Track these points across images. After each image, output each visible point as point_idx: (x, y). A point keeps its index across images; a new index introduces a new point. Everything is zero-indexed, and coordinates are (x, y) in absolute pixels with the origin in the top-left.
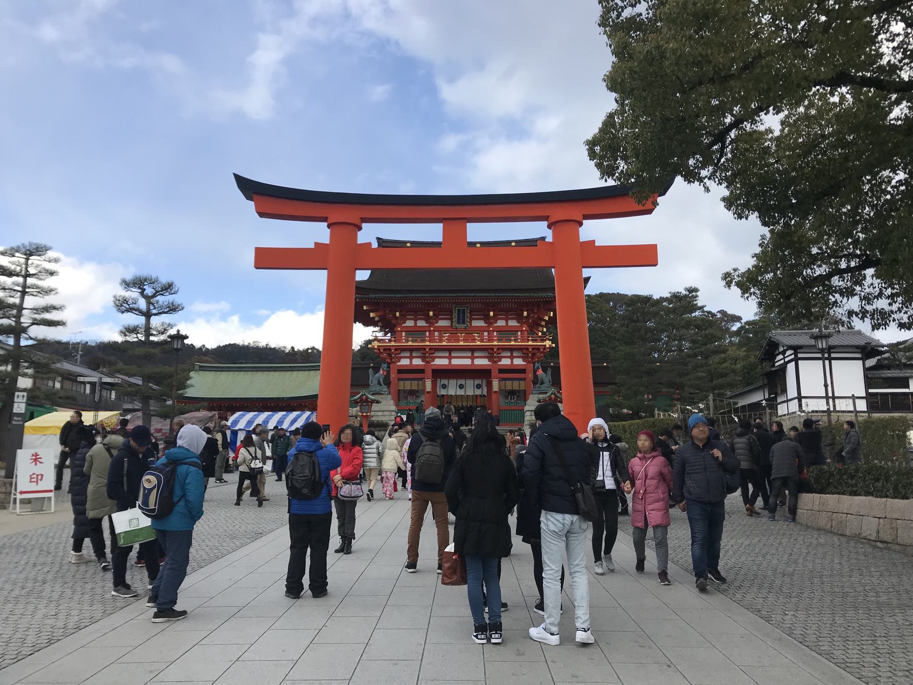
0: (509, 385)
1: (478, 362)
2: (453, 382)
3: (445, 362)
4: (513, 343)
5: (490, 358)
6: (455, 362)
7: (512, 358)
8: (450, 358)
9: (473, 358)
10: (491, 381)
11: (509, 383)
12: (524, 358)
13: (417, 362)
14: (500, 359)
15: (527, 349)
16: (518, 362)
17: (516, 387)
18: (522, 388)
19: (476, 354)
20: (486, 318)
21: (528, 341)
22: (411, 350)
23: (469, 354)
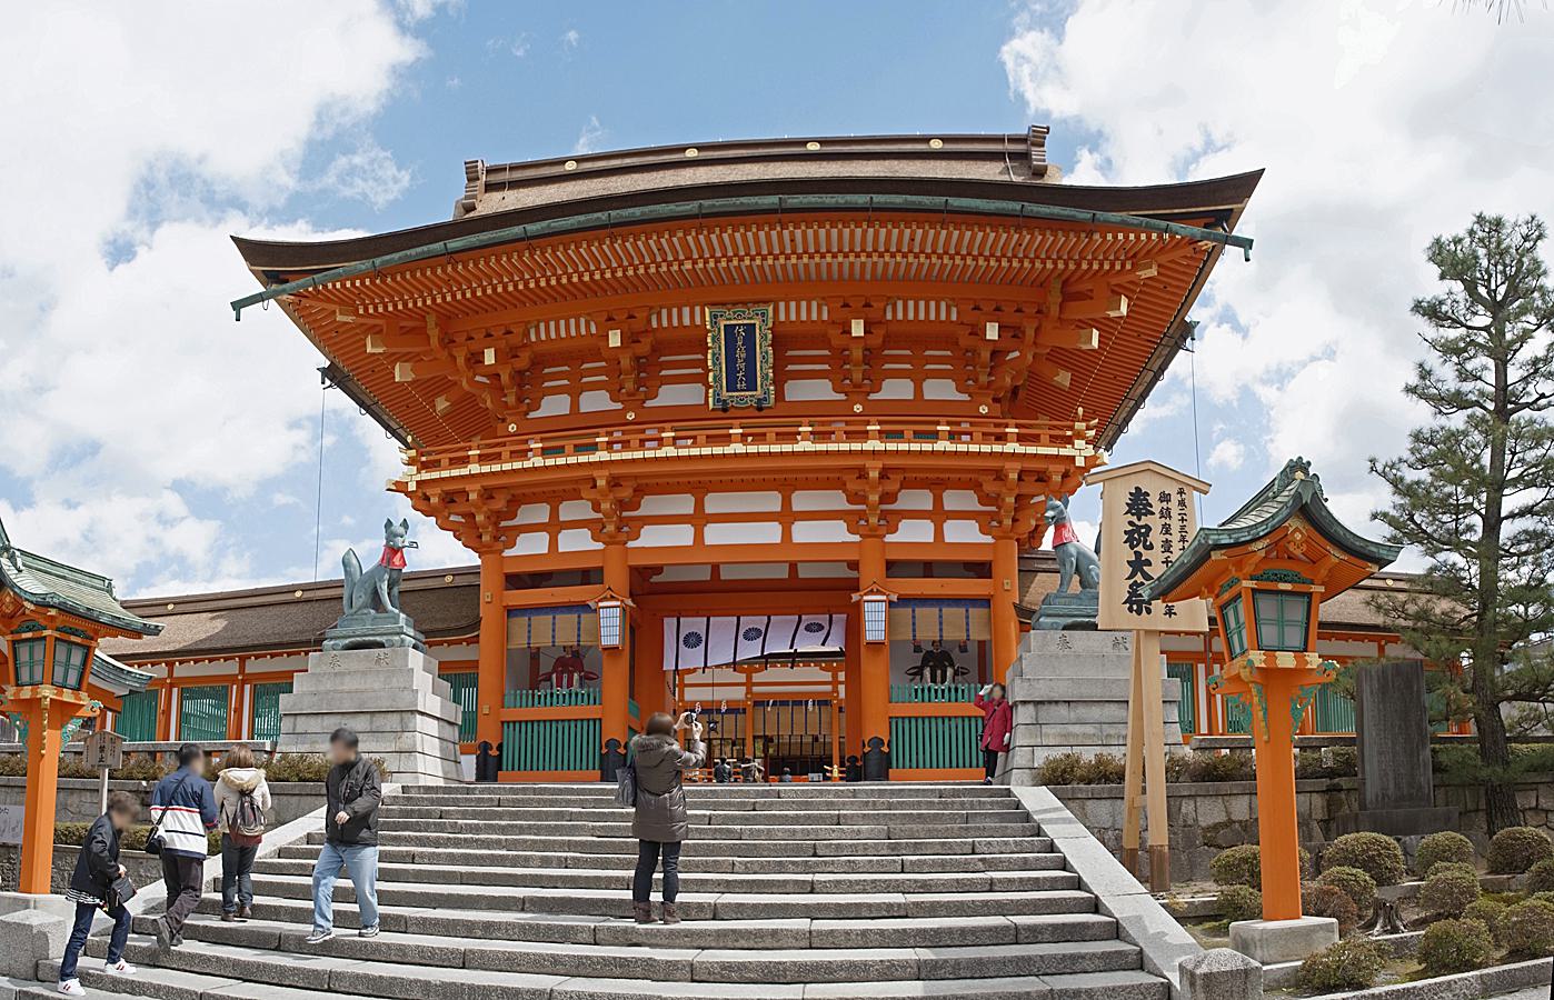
0: (928, 626)
1: (804, 533)
2: (723, 626)
3: (682, 536)
4: (941, 446)
5: (852, 520)
6: (716, 535)
7: (939, 515)
8: (699, 519)
9: (787, 517)
10: (858, 605)
11: (927, 614)
12: (985, 521)
13: (577, 542)
14: (891, 520)
15: (1000, 475)
16: (965, 533)
17: (953, 634)
18: (978, 634)
19: (802, 501)
20: (837, 369)
21: (1002, 438)
22: (553, 490)
23: (771, 501)
